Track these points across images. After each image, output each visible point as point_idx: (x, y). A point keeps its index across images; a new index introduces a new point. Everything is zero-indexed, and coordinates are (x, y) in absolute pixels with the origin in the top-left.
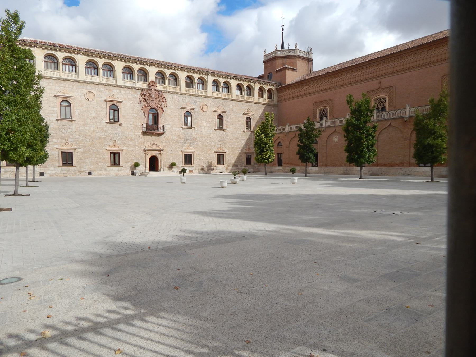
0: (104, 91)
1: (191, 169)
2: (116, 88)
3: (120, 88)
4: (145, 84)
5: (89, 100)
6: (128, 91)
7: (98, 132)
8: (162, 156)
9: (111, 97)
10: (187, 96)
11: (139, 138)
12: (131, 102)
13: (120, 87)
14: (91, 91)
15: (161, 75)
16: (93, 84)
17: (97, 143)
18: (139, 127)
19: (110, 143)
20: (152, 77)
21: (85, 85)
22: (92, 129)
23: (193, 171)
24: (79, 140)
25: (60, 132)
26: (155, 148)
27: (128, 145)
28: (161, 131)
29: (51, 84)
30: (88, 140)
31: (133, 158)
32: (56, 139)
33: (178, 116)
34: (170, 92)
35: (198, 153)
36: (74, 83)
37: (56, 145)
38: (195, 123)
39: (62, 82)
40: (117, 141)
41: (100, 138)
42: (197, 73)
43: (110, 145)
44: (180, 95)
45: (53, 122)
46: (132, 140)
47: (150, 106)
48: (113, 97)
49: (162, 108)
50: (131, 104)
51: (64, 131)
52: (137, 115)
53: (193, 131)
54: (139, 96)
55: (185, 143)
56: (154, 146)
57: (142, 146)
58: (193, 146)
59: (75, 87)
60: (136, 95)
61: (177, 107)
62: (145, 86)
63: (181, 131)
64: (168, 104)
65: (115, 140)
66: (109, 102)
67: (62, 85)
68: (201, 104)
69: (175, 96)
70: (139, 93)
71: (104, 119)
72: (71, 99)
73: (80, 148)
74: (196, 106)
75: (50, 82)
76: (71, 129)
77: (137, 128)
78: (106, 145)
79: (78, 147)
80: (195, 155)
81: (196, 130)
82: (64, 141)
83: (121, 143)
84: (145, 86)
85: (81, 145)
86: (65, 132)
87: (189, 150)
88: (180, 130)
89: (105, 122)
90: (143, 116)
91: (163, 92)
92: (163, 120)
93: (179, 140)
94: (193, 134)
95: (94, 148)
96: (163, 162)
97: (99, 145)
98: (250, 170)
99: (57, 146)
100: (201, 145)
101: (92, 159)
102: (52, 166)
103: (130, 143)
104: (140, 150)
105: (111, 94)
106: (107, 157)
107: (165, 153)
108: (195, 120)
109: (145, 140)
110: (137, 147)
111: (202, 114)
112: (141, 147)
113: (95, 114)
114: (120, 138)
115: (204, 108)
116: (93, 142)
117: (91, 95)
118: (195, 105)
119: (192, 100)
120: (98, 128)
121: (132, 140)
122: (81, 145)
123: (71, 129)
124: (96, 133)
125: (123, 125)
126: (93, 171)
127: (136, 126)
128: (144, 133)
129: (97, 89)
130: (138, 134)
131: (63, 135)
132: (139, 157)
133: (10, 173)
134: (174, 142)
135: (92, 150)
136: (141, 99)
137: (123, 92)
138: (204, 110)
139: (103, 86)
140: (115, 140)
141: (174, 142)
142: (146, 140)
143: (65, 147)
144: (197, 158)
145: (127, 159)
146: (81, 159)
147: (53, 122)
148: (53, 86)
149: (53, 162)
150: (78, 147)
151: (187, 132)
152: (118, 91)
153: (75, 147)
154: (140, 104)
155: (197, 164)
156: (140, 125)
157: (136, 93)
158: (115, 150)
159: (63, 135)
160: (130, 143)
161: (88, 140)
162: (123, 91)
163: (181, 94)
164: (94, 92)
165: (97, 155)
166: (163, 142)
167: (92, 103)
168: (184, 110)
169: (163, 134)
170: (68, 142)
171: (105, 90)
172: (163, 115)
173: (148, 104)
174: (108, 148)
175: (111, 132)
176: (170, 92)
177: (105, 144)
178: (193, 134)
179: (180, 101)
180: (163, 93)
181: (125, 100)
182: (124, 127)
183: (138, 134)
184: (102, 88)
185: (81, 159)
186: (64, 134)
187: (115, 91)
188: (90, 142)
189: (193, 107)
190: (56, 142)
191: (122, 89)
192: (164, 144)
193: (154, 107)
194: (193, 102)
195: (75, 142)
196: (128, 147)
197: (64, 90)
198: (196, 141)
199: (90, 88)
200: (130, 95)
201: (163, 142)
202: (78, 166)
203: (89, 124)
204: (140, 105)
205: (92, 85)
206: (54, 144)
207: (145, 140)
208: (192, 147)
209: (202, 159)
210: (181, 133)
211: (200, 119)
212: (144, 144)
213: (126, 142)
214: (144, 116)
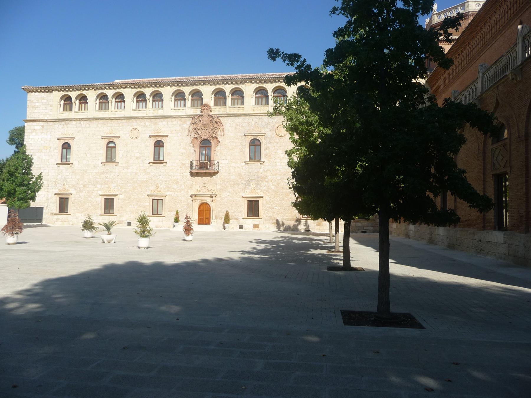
0: (150, 125)
1: (256, 223)
2: (162, 120)
3: (167, 119)
4: (197, 110)
5: (133, 138)
6: (176, 122)
7: (141, 175)
8: (214, 203)
9: (156, 131)
10: (255, 117)
11: (185, 180)
12: (179, 135)
13: (166, 118)
14: (136, 127)
15: (219, 94)
16: (138, 119)
17: (138, 188)
18: (187, 165)
19: (153, 188)
20: (208, 98)
21: (131, 121)
22: (135, 171)
23: (260, 226)
24: (121, 185)
25: (104, 177)
26: (204, 192)
27: (172, 190)
28: (214, 169)
29: (100, 126)
30: (130, 184)
31: (178, 206)
32: (100, 184)
33: (240, 147)
34: (228, 115)
35: (268, 199)
36: (119, 121)
37: (100, 191)
38: (266, 155)
39: (110, 121)
40: (159, 185)
41: (142, 182)
42: (270, 81)
43: (152, 190)
44: (243, 117)
45: (98, 167)
46: (177, 183)
47: (202, 137)
48: (158, 131)
49: (216, 138)
50: (178, 137)
51: (108, 175)
52: (184, 150)
53: (263, 166)
54: (189, 126)
55: (248, 183)
56: (205, 190)
57: (189, 191)
58: (261, 188)
59: (121, 125)
60: (185, 126)
61: (239, 134)
62: (197, 111)
63: (244, 168)
64: (226, 131)
65: (157, 184)
66: (153, 138)
67: (109, 125)
68: (277, 126)
69: (237, 120)
70: (189, 121)
71: (147, 159)
72: (115, 139)
73: (122, 194)
74: (268, 130)
75: (99, 123)
76: (114, 172)
77: (183, 167)
78: (148, 190)
79: (119, 193)
80: (264, 202)
81: (267, 164)
82: (107, 186)
83: (165, 187)
84: (197, 111)
85: (123, 190)
86: (109, 177)
87: (254, 195)
88: (242, 166)
89: (148, 162)
90: (192, 151)
91: (219, 117)
92: (219, 154)
93: (240, 180)
94: (261, 170)
95: (135, 194)
96: (216, 212)
97: (140, 190)
98: (365, 228)
99: (100, 192)
100: (273, 187)
101: (133, 207)
102: (95, 214)
103: (175, 187)
104: (186, 196)
105: (157, 128)
106: (148, 204)
107: (218, 198)
108: (265, 150)
109: (193, 182)
110: (183, 192)
111: (278, 141)
112: (187, 191)
113: (138, 154)
114: (163, 181)
115: (281, 131)
116: (135, 187)
117: (136, 131)
118: (267, 128)
119: (262, 122)
120: (140, 170)
121: (177, 183)
122: (123, 190)
123: (114, 172)
124: (138, 175)
125: (168, 164)
126: (132, 221)
127: (183, 164)
128: (192, 174)
129: (142, 124)
130: (185, 174)
131: (107, 180)
132: (185, 205)
133: (61, 220)
134: (233, 183)
135: (133, 196)
136: (191, 129)
137: (170, 123)
138: (281, 134)
139: (149, 120)
140: (157, 184)
141: (233, 183)
142: (194, 182)
143: (107, 193)
144: (268, 207)
145: (171, 207)
146: (122, 207)
147: (98, 167)
148: (101, 127)
149: (96, 209)
150: (119, 193)
151: (252, 168)
152: (164, 123)
153: (117, 193)
154: (189, 136)
155: (267, 216)
156: (188, 163)
157: (185, 122)
158: (157, 196)
159: (107, 180)
160: (175, 187)
161: (130, 184)
162: (170, 122)
163: (245, 115)
164: (139, 129)
165: (138, 202)
166: (217, 185)
167: (136, 140)
168: (249, 137)
169: (217, 173)
170: (110, 187)
171: (151, 124)
172: (219, 148)
173: (199, 134)
174: (149, 193)
175: (153, 173)
176: (228, 115)
177: (147, 189)
178: (261, 170)
179: (244, 126)
180: (220, 118)
181: (172, 133)
182: (169, 167)
183: (185, 174)
184: (147, 122)
185: (122, 207)
186: (107, 178)
187: (162, 123)
188: (131, 187)
189: (263, 132)
190: (100, 187)
191: (170, 119)
192: (219, 187)
193: (206, 137)
194: (264, 124)
195: (117, 188)
196: (172, 191)
197: (111, 130)
198: (266, 181)
199: (135, 123)
200: (178, 126)
201: (217, 185)
202: (118, 215)
203: (132, 166)
204: (189, 137)
205: (138, 121)
206: (98, 190)
207: (193, 182)
208: (259, 191)
209: (275, 207)
210: (242, 170)
211: (274, 148)
212: (191, 188)
213: (170, 186)
214: (194, 151)
